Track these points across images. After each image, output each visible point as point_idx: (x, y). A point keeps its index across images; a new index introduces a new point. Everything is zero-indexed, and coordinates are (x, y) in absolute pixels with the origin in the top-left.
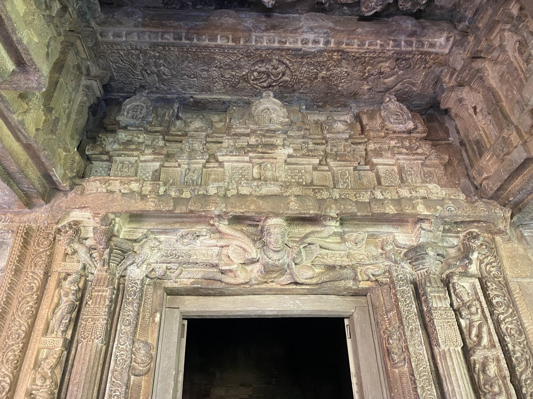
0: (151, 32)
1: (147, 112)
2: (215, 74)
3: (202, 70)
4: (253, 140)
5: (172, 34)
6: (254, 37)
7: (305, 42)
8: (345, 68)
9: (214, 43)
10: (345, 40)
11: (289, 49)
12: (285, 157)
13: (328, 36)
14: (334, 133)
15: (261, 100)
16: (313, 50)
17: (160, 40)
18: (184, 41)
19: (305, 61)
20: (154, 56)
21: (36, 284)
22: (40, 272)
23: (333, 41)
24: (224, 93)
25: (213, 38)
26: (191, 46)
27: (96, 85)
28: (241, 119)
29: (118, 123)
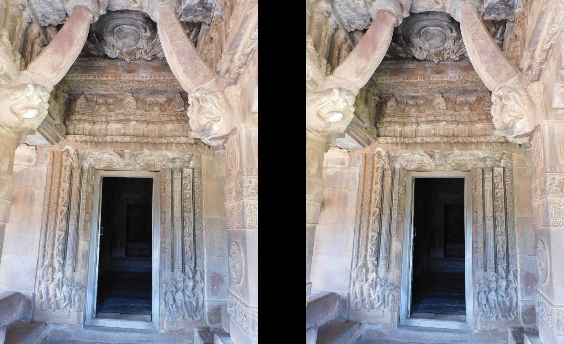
8: (159, 85)
21: (59, 168)
22: (59, 165)
27: (67, 95)
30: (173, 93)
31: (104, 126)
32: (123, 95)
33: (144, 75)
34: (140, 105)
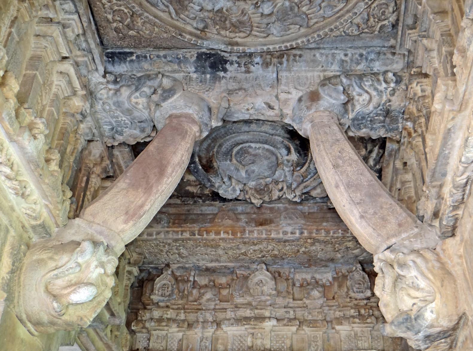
0: (174, 231)
1: (172, 291)
2: (221, 252)
3: (211, 251)
4: (248, 313)
5: (188, 232)
6: (247, 232)
7: (285, 233)
9: (219, 237)
10: (315, 231)
11: (273, 239)
12: (270, 328)
13: (302, 229)
14: (311, 300)
15: (256, 273)
16: (292, 238)
17: (180, 236)
18: (197, 236)
19: (287, 244)
20: (176, 246)
23: (305, 231)
24: (228, 262)
25: (218, 233)
26: (202, 240)
27: (135, 271)
28: (241, 290)
29: (152, 300)
30: (347, 263)
31: (210, 331)
32: (249, 268)
33: (288, 229)
34: (282, 286)
